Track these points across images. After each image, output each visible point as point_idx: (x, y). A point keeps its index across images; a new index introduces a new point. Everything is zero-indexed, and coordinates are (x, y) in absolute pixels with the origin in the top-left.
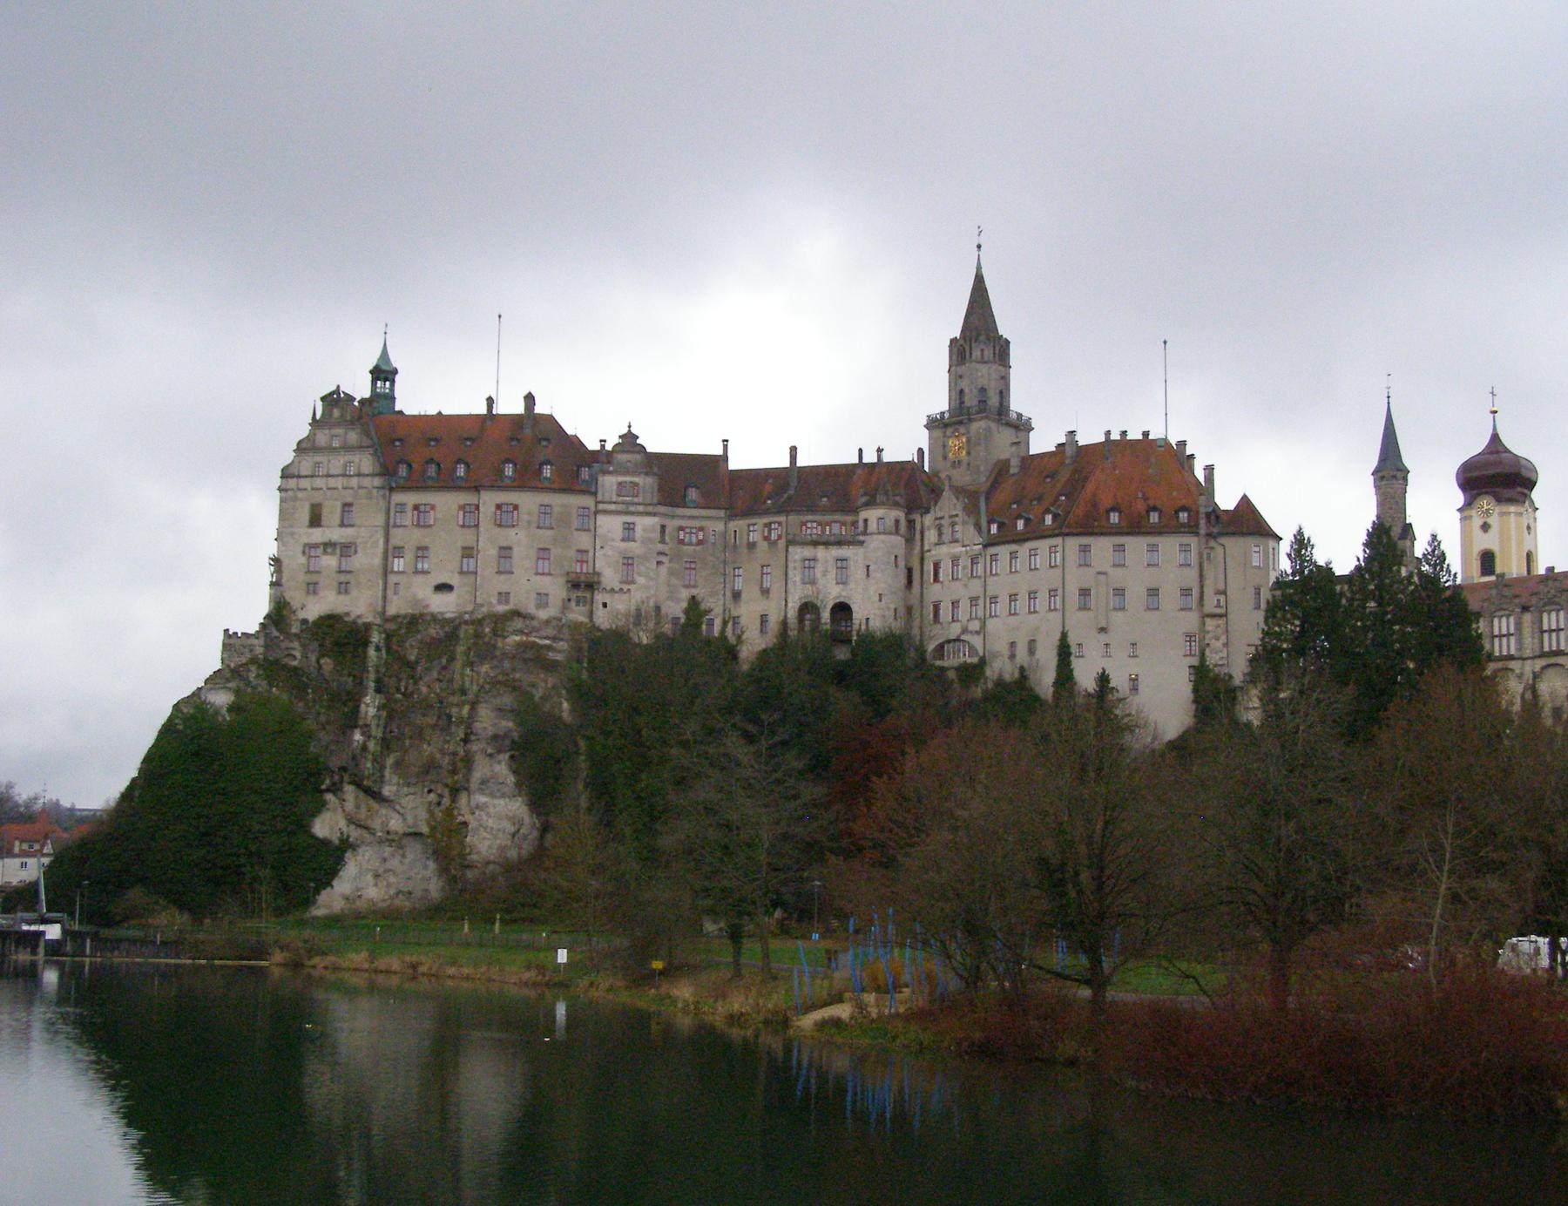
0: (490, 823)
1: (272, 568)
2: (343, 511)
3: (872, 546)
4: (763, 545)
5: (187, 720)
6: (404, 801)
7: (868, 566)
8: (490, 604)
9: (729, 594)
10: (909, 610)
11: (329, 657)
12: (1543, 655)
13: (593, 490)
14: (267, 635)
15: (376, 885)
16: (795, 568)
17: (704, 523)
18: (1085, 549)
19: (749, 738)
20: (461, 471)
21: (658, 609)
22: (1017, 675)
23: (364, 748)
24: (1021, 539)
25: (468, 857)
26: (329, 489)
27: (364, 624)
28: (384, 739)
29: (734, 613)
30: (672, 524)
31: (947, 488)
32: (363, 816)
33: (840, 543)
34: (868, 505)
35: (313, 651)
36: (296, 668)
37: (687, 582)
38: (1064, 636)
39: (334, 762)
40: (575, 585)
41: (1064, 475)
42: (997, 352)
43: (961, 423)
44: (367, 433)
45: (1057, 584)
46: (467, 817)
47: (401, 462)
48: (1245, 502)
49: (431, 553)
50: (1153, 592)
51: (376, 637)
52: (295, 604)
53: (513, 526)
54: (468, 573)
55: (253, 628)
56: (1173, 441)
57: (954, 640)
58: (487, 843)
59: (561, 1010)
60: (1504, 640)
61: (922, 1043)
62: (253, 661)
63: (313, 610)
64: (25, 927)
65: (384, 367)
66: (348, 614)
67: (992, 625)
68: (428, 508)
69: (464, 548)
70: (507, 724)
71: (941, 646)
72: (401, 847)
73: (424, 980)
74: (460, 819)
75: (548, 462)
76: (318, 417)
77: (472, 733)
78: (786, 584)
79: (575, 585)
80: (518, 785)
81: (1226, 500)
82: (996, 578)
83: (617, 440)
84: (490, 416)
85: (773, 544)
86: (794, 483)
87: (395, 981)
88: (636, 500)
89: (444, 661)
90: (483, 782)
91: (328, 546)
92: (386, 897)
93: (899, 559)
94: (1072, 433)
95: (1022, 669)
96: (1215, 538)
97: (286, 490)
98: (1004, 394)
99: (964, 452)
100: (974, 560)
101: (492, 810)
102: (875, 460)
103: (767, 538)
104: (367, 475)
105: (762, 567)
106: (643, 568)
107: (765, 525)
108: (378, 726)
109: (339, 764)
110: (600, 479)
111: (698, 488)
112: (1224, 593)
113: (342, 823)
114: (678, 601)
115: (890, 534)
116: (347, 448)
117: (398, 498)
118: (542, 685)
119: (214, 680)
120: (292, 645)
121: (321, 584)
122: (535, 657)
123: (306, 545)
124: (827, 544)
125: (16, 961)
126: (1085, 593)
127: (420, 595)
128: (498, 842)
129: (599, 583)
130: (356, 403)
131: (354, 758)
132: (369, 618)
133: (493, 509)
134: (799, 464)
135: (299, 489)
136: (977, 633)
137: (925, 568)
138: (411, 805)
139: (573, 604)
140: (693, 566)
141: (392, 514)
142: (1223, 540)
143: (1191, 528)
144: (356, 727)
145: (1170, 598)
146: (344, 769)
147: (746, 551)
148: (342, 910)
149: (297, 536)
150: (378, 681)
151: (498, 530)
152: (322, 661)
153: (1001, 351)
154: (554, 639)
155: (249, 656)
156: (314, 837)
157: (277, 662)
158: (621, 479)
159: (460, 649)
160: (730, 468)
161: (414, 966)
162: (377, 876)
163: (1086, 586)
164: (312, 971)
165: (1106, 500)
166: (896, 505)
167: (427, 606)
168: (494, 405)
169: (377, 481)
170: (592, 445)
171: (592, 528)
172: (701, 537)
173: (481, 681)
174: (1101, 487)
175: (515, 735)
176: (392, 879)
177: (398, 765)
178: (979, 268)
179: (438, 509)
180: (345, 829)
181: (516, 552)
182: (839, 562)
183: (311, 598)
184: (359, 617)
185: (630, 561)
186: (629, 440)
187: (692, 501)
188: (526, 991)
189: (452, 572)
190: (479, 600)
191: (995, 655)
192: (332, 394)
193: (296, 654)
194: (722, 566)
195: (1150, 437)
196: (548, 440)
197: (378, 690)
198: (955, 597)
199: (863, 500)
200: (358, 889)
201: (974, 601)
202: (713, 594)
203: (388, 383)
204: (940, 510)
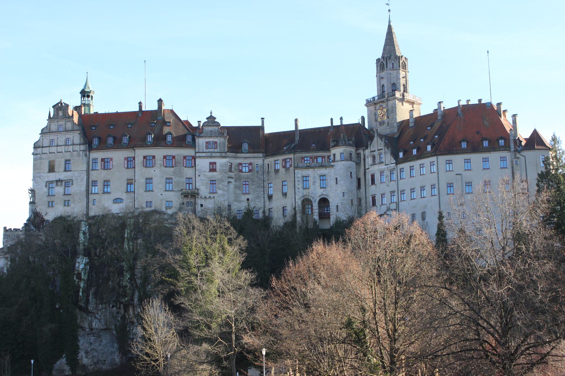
1: (30, 195)
2: (66, 164)
4: (282, 171)
7: (336, 179)
10: (360, 200)
15: (86, 357)
21: (229, 206)
26: (58, 152)
28: (88, 280)
31: (376, 135)
33: (322, 166)
37: (244, 192)
40: (186, 195)
41: (437, 125)
49: (111, 183)
51: (84, 228)
53: (153, 167)
56: (494, 104)
63: (50, 215)
65: (86, 90)
66: (69, 216)
69: (128, 180)
76: (52, 116)
78: (295, 190)
83: (206, 120)
85: (287, 169)
86: (297, 138)
88: (216, 150)
91: (58, 181)
92: (92, 363)
93: (352, 173)
94: (440, 103)
97: (36, 154)
99: (386, 117)
100: (391, 173)
102: (339, 124)
103: (284, 167)
104: (77, 145)
106: (220, 186)
107: (283, 160)
108: (85, 274)
110: (197, 140)
115: (347, 160)
123: (47, 182)
124: (313, 168)
126: (450, 185)
129: (198, 194)
133: (142, 159)
136: (394, 210)
137: (367, 178)
139: (185, 205)
140: (247, 183)
143: (506, 148)
149: (42, 178)
151: (144, 169)
158: (208, 140)
163: (450, 182)
166: (350, 145)
167: (110, 210)
169: (82, 147)
170: (195, 124)
172: (251, 168)
179: (114, 160)
181: (155, 181)
182: (322, 177)
183: (50, 209)
184: (75, 217)
186: (211, 120)
192: (58, 103)
195: (482, 102)
201: (392, 193)
202: (258, 197)
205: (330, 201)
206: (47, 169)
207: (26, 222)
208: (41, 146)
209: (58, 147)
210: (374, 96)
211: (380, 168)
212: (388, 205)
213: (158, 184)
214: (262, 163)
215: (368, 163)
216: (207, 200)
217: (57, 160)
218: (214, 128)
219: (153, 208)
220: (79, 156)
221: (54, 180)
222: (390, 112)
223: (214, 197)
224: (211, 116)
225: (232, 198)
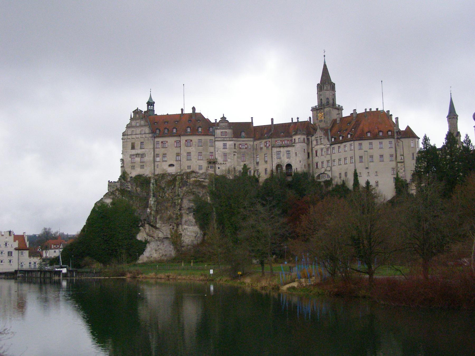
0: (188, 234)
3: (297, 147)
4: (265, 148)
5: (99, 207)
6: (163, 228)
7: (296, 153)
8: (185, 170)
10: (309, 165)
11: (139, 187)
14: (121, 182)
15: (156, 253)
16: (274, 154)
18: (360, 144)
19: (263, 205)
21: (235, 168)
22: (342, 183)
23: (151, 213)
24: (341, 142)
25: (182, 244)
26: (136, 138)
27: (149, 177)
28: (156, 210)
29: (257, 169)
30: (237, 143)
31: (318, 128)
32: (151, 233)
33: (287, 146)
36: (129, 191)
37: (243, 160)
38: (355, 170)
40: (210, 163)
41: (353, 123)
42: (331, 87)
43: (322, 109)
44: (147, 121)
45: (353, 155)
46: (182, 232)
47: (157, 129)
48: (408, 127)
49: (167, 155)
50: (381, 156)
51: (152, 181)
52: (128, 172)
53: (191, 146)
54: (178, 161)
55: (116, 180)
56: (385, 111)
57: (323, 173)
59: (212, 288)
61: (319, 293)
62: (117, 189)
63: (134, 174)
64: (56, 270)
65: (151, 102)
66: (144, 174)
67: (333, 168)
68: (166, 142)
69: (177, 153)
70: (192, 204)
71: (319, 175)
72: (163, 242)
73: (171, 280)
74: (179, 233)
75: (200, 127)
76: (132, 117)
77: (182, 207)
80: (196, 222)
81: (402, 127)
84: (182, 115)
85: (267, 148)
86: (273, 130)
87: (163, 281)
88: (226, 137)
89: (173, 187)
90: (186, 222)
91: (137, 155)
94: (355, 110)
95: (343, 181)
96: (399, 139)
97: (124, 139)
98: (334, 100)
99: (323, 117)
101: (188, 230)
103: (265, 146)
104: (148, 133)
105: (265, 154)
106: (229, 157)
107: (265, 142)
108: (154, 207)
109: (143, 218)
111: (244, 132)
112: (403, 155)
113: (145, 236)
114: (240, 166)
115: (302, 143)
116: (141, 126)
117: (157, 140)
118: (201, 192)
119: (106, 196)
121: (136, 166)
122: (199, 184)
123: (131, 155)
124: (284, 147)
126: (361, 157)
127: (165, 168)
128: (191, 239)
129: (217, 162)
130: (143, 113)
131: (148, 216)
132: (150, 175)
133: (185, 141)
141: (155, 145)
142: (402, 140)
143: (392, 136)
144: (148, 207)
145: (387, 158)
146: (145, 220)
147: (259, 150)
148: (146, 261)
149: (128, 152)
150: (153, 193)
151: (186, 148)
152: (137, 189)
153: (333, 86)
154: (204, 179)
155: (116, 188)
156: (137, 240)
157: (124, 189)
158: (222, 131)
159: (177, 183)
160: (254, 126)
161: (168, 276)
162: (156, 251)
163: (361, 155)
164: (138, 279)
165: (366, 130)
166: (304, 134)
167: (167, 171)
168: (183, 111)
169: (150, 135)
170: (213, 121)
171: (214, 146)
172: (246, 147)
173: (184, 192)
174: (364, 126)
175: (195, 207)
176: (161, 251)
177: (161, 218)
178: (325, 62)
179: (168, 142)
181: (192, 154)
182: (287, 152)
184: (147, 175)
185: (226, 155)
186: (224, 119)
188: (201, 282)
191: (335, 177)
192: (136, 110)
193: (130, 187)
194: (253, 155)
195: (379, 110)
197: (154, 196)
198: (322, 161)
199: (293, 133)
200: (151, 255)
202: (251, 163)
203: (152, 106)
205: (292, 166)
207: (119, 178)
208: (127, 134)
209: (136, 135)
210: (316, 105)
211: (321, 147)
212: (326, 168)
213: (194, 155)
214: (253, 144)
215: (314, 144)
216: (222, 165)
220: (148, 140)
221: (135, 154)
222: (325, 114)
223: (226, 163)
224: (224, 116)
225: (236, 164)
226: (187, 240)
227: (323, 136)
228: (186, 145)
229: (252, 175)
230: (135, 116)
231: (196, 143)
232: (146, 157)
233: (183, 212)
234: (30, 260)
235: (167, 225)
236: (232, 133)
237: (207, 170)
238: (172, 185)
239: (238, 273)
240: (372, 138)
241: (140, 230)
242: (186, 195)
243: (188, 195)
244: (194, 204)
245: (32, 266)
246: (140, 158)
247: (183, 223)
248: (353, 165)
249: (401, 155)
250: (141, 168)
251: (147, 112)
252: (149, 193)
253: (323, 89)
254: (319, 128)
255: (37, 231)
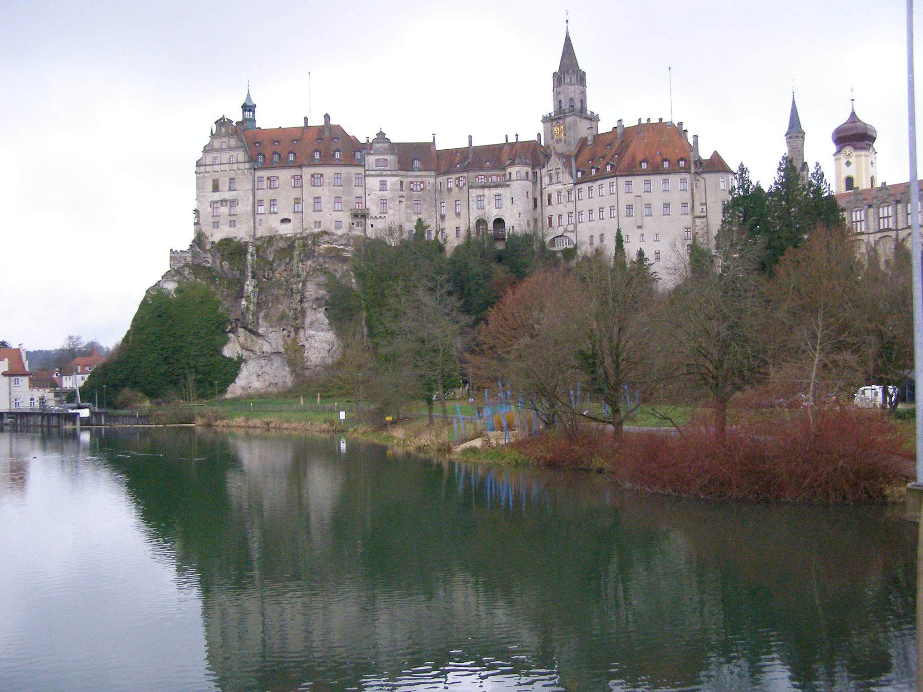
0: (316, 345)
2: (230, 183)
4: (456, 190)
6: (270, 336)
8: (311, 228)
9: (438, 217)
10: (536, 220)
11: (226, 261)
12: (880, 231)
13: (363, 164)
14: (193, 251)
15: (258, 381)
16: (473, 201)
17: (424, 179)
18: (629, 183)
19: (432, 290)
20: (291, 157)
23: (248, 308)
24: (594, 180)
25: (306, 364)
28: (258, 303)
29: (441, 227)
30: (406, 181)
31: (553, 154)
32: (249, 345)
33: (497, 186)
34: (510, 165)
35: (218, 258)
36: (209, 268)
38: (619, 231)
39: (232, 317)
40: (356, 216)
41: (617, 144)
43: (560, 118)
44: (241, 141)
46: (305, 343)
47: (260, 154)
48: (716, 153)
50: (666, 205)
51: (251, 249)
52: (208, 234)
53: (321, 186)
54: (298, 212)
55: (186, 247)
56: (676, 123)
57: (560, 236)
58: (315, 356)
59: (343, 446)
60: (859, 223)
61: (517, 461)
62: (187, 265)
63: (217, 236)
64: (70, 411)
65: (249, 104)
66: (235, 238)
67: (579, 226)
68: (275, 179)
70: (322, 292)
71: (554, 239)
72: (270, 360)
73: (273, 430)
75: (338, 150)
76: (214, 132)
77: (304, 297)
79: (356, 216)
80: (330, 324)
81: (705, 154)
82: (582, 201)
83: (376, 137)
85: (461, 189)
86: (471, 155)
87: (258, 431)
88: (386, 168)
90: (311, 324)
91: (223, 202)
96: (700, 174)
97: (199, 173)
98: (583, 102)
102: (515, 141)
103: (457, 186)
106: (391, 205)
107: (456, 179)
108: (254, 296)
112: (705, 204)
113: (239, 349)
114: (412, 222)
115: (524, 180)
116: (231, 149)
117: (259, 174)
118: (340, 270)
119: (167, 276)
120: (206, 256)
121: (221, 222)
122: (335, 255)
123: (211, 202)
124: (489, 187)
125: (65, 429)
126: (629, 207)
127: (273, 226)
128: (321, 355)
129: (368, 214)
130: (234, 124)
131: (243, 314)
132: (247, 239)
134: (473, 145)
135: (206, 172)
138: (274, 338)
139: (355, 226)
141: (256, 183)
142: (704, 176)
143: (687, 170)
144: (242, 297)
145: (676, 208)
146: (237, 320)
148: (241, 394)
150: (253, 272)
151: (312, 188)
152: (223, 264)
153: (581, 78)
154: (346, 245)
155: (184, 262)
156: (223, 356)
157: (199, 265)
158: (377, 157)
159: (296, 253)
160: (437, 149)
161: (268, 424)
162: (258, 376)
163: (630, 203)
164: (216, 427)
165: (640, 157)
166: (526, 164)
167: (278, 231)
169: (247, 166)
171: (363, 185)
172: (422, 187)
173: (308, 269)
174: (637, 149)
175: (327, 297)
176: (267, 377)
178: (567, 33)
180: (240, 352)
181: (323, 200)
184: (241, 239)
186: (381, 135)
187: (416, 167)
188: (323, 435)
189: (290, 212)
190: (304, 227)
191: (583, 243)
192: (221, 119)
193: (209, 260)
195: (663, 121)
196: (338, 138)
197: (253, 277)
198: (560, 213)
199: (508, 162)
200: (249, 383)
201: (570, 214)
202: (430, 217)
203: (251, 113)
204: (550, 165)
206: (211, 188)
212: (565, 226)
213: (327, 203)
216: (378, 220)
217: (221, 179)
218: (384, 144)
219: (322, 229)
220: (244, 174)
221: (219, 199)
225: (403, 219)
226: (315, 356)
227: (561, 168)
228: (313, 184)
229: (433, 238)
230: (218, 130)
231: (330, 179)
232: (239, 205)
233: (306, 305)
234: (32, 393)
235: (277, 329)
236: (397, 162)
237: (350, 229)
238: (287, 256)
239: (387, 420)
240: (650, 172)
241: (228, 339)
242: (313, 275)
243: (315, 275)
244: (327, 291)
245: (37, 405)
246: (229, 207)
247: (306, 326)
248: (614, 221)
249: (702, 204)
250: (231, 226)
251: (242, 124)
252: (244, 271)
253: (563, 82)
254: (555, 153)
255: (54, 342)
